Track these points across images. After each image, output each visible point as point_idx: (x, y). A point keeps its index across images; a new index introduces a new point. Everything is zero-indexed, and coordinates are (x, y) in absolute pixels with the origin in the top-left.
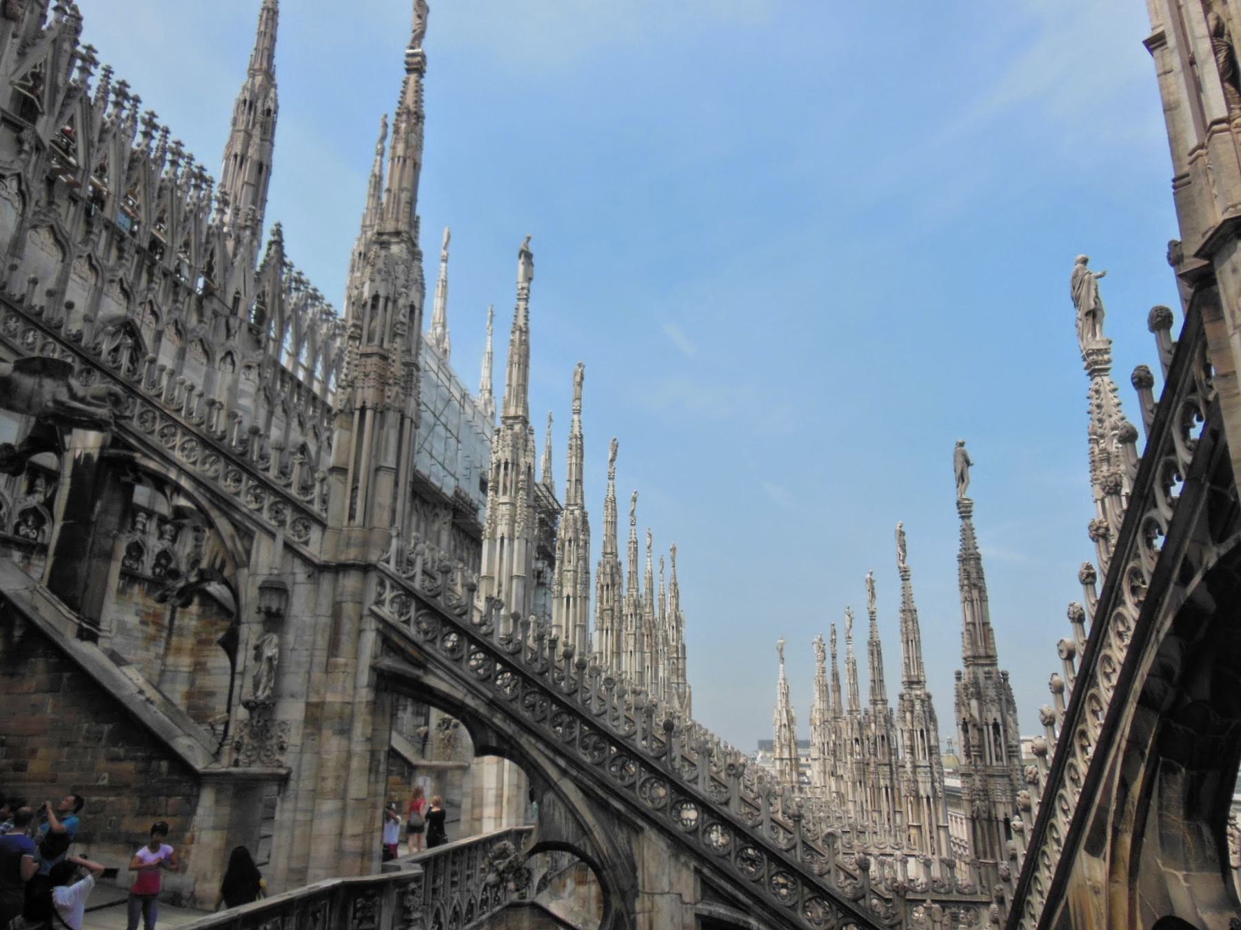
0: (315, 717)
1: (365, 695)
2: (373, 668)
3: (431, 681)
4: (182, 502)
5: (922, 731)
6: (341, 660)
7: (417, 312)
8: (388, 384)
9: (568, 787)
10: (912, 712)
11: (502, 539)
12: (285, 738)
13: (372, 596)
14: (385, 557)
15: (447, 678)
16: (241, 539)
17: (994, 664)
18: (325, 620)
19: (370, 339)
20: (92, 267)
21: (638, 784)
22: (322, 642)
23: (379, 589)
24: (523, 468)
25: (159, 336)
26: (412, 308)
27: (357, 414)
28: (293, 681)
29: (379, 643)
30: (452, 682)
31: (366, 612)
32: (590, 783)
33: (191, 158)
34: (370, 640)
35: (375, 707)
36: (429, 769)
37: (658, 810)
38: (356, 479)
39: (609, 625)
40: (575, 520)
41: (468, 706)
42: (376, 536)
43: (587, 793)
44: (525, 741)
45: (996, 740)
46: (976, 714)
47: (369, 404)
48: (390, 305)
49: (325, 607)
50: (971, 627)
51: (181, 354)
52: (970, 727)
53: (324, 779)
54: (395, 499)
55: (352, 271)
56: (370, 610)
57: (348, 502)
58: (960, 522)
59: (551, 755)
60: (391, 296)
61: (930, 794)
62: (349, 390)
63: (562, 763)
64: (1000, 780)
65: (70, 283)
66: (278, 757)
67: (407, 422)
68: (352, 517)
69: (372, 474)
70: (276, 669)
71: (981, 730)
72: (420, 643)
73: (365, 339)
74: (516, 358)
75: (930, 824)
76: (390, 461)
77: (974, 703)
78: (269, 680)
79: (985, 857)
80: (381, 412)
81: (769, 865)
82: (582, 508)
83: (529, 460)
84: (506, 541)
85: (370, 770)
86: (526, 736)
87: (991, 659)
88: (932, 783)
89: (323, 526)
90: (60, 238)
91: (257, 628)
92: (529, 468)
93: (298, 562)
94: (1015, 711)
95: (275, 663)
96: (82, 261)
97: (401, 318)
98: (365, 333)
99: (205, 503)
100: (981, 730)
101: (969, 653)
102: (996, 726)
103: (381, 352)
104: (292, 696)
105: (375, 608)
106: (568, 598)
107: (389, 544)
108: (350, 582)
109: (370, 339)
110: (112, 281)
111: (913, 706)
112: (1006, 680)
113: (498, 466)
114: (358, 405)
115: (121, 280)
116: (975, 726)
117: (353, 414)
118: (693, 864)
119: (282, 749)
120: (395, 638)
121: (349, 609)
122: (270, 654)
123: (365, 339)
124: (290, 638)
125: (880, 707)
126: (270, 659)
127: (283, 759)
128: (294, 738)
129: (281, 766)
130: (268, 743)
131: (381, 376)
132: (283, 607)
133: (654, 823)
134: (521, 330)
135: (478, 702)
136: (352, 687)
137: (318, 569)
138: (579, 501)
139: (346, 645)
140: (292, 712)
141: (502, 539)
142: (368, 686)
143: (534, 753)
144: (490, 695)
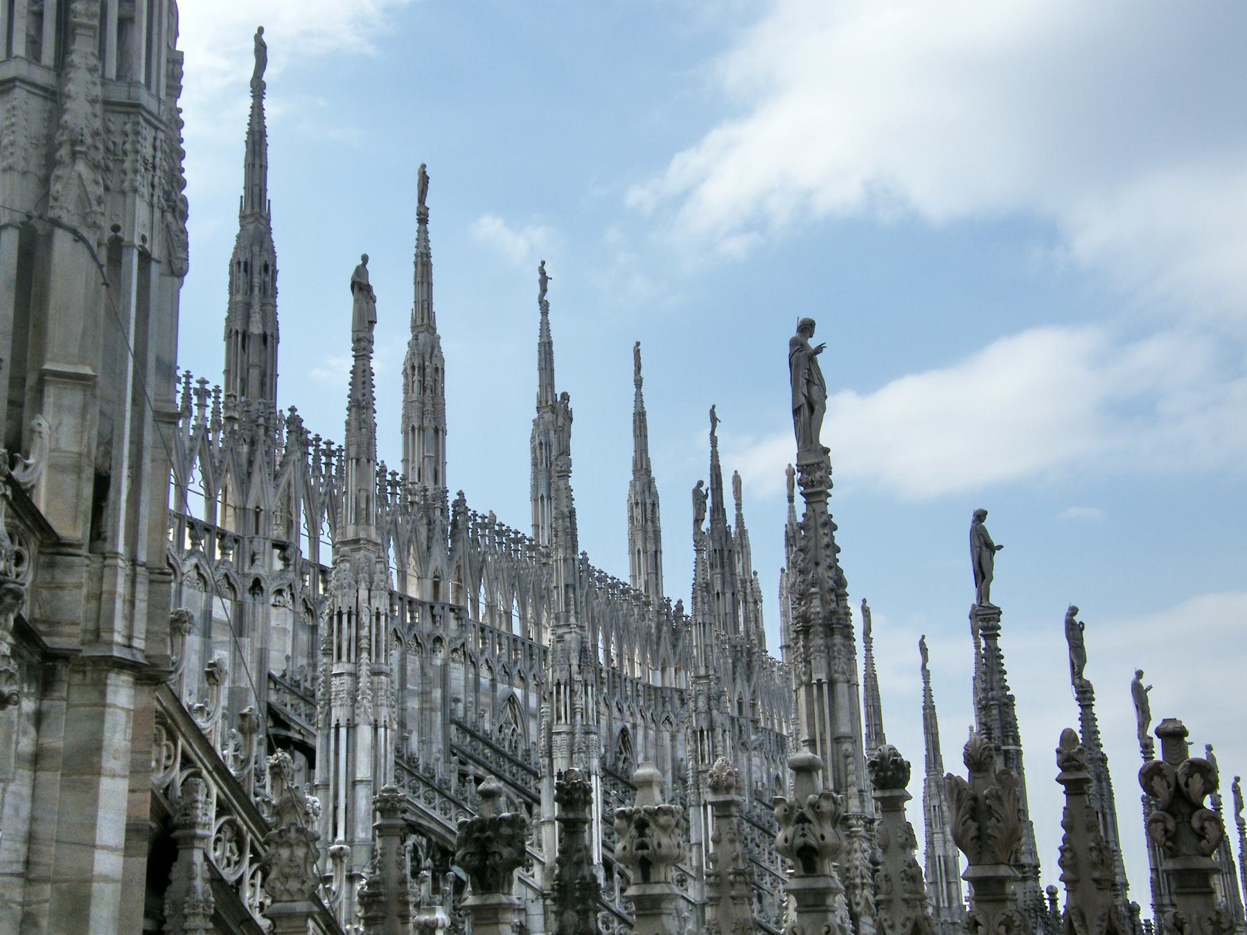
84: (343, 731)
141: (337, 727)
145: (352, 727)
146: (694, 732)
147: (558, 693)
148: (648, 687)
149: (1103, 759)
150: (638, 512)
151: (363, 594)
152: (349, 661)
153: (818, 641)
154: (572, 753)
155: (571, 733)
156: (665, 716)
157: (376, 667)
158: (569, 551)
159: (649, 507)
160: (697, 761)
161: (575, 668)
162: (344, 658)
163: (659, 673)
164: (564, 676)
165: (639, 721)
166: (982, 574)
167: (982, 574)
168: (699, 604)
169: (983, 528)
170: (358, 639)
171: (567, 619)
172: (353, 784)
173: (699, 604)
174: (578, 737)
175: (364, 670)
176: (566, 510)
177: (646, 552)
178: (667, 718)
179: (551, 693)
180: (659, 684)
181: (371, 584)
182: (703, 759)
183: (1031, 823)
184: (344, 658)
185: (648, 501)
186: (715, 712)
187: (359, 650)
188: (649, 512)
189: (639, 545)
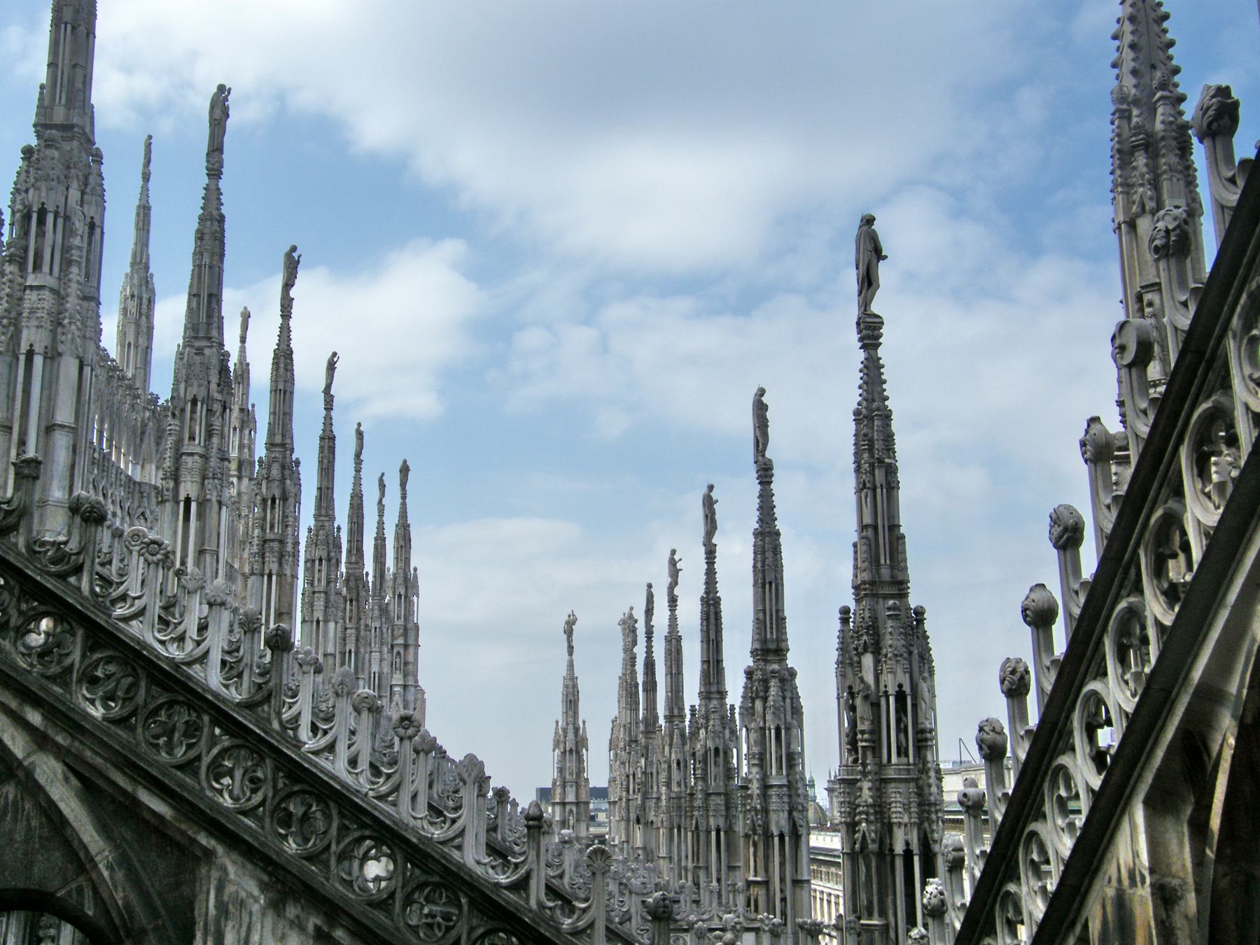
5: (778, 730)
10: (765, 699)
17: (903, 595)
21: (206, 761)
37: (245, 813)
39: (274, 567)
45: (898, 721)
46: (870, 678)
50: (870, 533)
52: (858, 701)
58: (861, 355)
59: (14, 704)
61: (786, 830)
64: (902, 788)
71: (876, 706)
75: (782, 880)
77: (868, 660)
79: (870, 916)
81: (469, 919)
83: (90, 211)
84: (38, 361)
87: (900, 587)
88: (790, 813)
94: (931, 673)
100: (876, 706)
101: (865, 576)
102: (900, 697)
106: (188, 501)
111: (767, 689)
112: (920, 621)
116: (866, 697)
118: (313, 921)
125: (714, 703)
133: (233, 840)
141: (30, 354)
145: (52, 356)
146: (264, 501)
147: (193, 411)
148: (130, 479)
149: (778, 534)
150: (132, 306)
151: (74, 195)
152: (51, 273)
153: (1168, 159)
154: (204, 478)
155: (205, 457)
156: (141, 510)
157: (87, 290)
158: (216, 258)
159: (145, 301)
160: (263, 529)
161: (213, 386)
162: (46, 269)
163: (139, 468)
164: (202, 394)
165: (119, 512)
166: (868, 282)
167: (868, 282)
168: (282, 371)
169: (874, 231)
170: (66, 249)
171: (208, 331)
172: (49, 429)
173: (282, 371)
174: (214, 462)
175: (73, 289)
176: (215, 213)
177: (136, 347)
178: (143, 514)
179: (183, 410)
180: (138, 480)
181: (86, 184)
182: (272, 527)
183: (903, 537)
184: (46, 269)
185: (145, 296)
186: (288, 482)
187: (67, 263)
188: (144, 306)
189: (131, 338)
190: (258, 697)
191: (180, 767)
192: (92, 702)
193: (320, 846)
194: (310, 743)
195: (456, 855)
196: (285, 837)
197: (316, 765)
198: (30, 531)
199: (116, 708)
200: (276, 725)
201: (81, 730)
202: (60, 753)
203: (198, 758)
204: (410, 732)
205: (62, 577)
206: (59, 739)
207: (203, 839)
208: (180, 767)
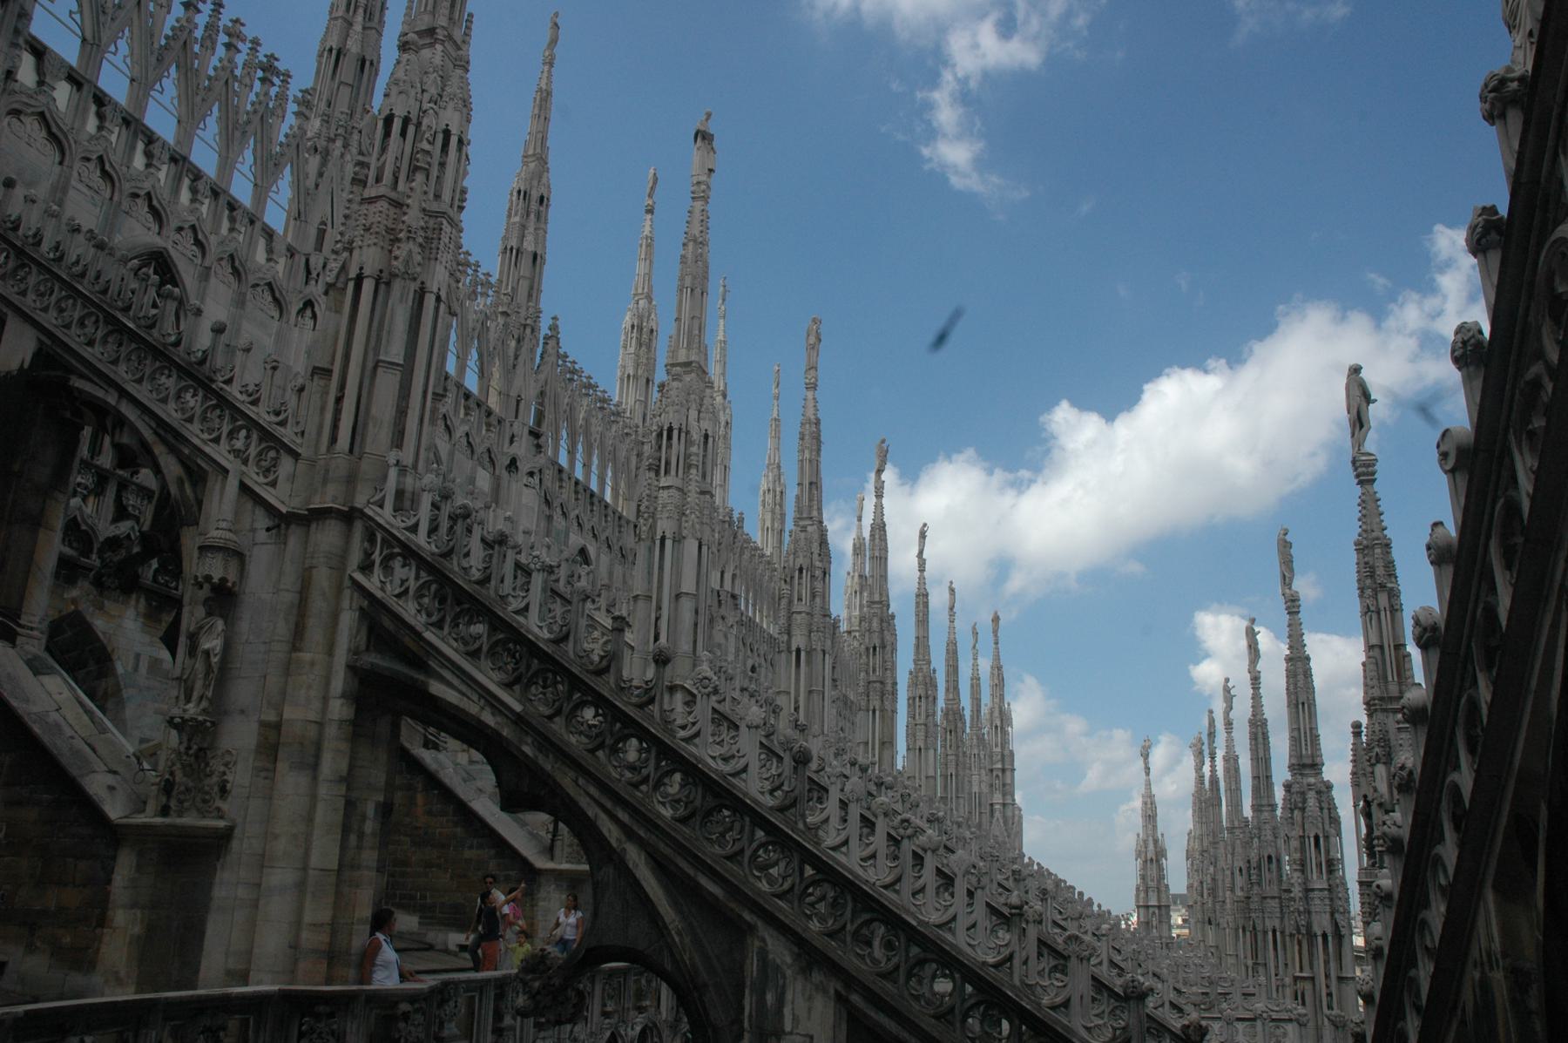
0: (271, 743)
1: (339, 709)
2: (351, 668)
3: (437, 688)
4: (125, 439)
6: (306, 656)
7: (454, 140)
8: (399, 240)
9: (635, 858)
11: (663, 539)
12: (229, 777)
13: (355, 558)
14: (377, 498)
15: (456, 682)
16: (194, 485)
18: (289, 597)
19: (378, 180)
20: (105, 175)
22: (283, 629)
23: (366, 544)
24: (696, 436)
25: (206, 274)
26: (447, 133)
27: (351, 285)
28: (243, 692)
29: (364, 633)
30: (463, 688)
31: (347, 583)
32: (668, 851)
33: (256, 43)
34: (348, 619)
35: (358, 730)
36: (558, 875)
37: (779, 896)
38: (342, 387)
40: (809, 541)
41: (487, 726)
42: (366, 466)
43: (660, 866)
44: (566, 780)
47: (366, 272)
48: (411, 129)
49: (290, 580)
51: (240, 302)
53: (276, 837)
54: (402, 413)
55: (509, 216)
56: (351, 578)
57: (329, 416)
60: (414, 116)
62: (346, 254)
63: (623, 816)
65: (71, 193)
66: (219, 803)
67: (430, 301)
68: (334, 439)
69: (368, 373)
70: (222, 673)
72: (419, 628)
73: (371, 180)
74: (688, 281)
76: (395, 351)
78: (206, 687)
80: (384, 281)
82: (821, 522)
85: (346, 830)
86: (572, 774)
89: (296, 456)
90: (54, 130)
91: (200, 612)
92: (706, 436)
93: (260, 513)
95: (215, 660)
96: (91, 166)
97: (426, 146)
98: (372, 174)
99: (148, 435)
103: (393, 195)
104: (242, 712)
105: (359, 577)
107: (385, 477)
108: (327, 536)
109: (378, 180)
110: (135, 196)
113: (660, 435)
114: (353, 274)
115: (100, 158)
117: (344, 289)
119: (224, 791)
120: (387, 622)
121: (322, 578)
122: (207, 646)
123: (371, 180)
124: (244, 626)
126: (207, 653)
127: (224, 806)
128: (241, 777)
129: (221, 818)
130: (207, 781)
131: (389, 230)
132: (232, 577)
134: (695, 241)
135: (499, 719)
136: (319, 697)
137: (282, 521)
138: (815, 513)
139: (315, 632)
140: (239, 736)
142: (343, 696)
143: (584, 802)
144: (518, 708)
190: (787, 802)
191: (728, 858)
192: (663, 804)
193: (836, 927)
194: (830, 838)
195: (949, 937)
196: (809, 917)
197: (834, 859)
198: (619, 671)
199: (681, 812)
200: (801, 826)
201: (657, 826)
202: (642, 844)
203: (742, 851)
204: (909, 831)
205: (641, 706)
206: (642, 833)
207: (747, 916)
208: (728, 858)
